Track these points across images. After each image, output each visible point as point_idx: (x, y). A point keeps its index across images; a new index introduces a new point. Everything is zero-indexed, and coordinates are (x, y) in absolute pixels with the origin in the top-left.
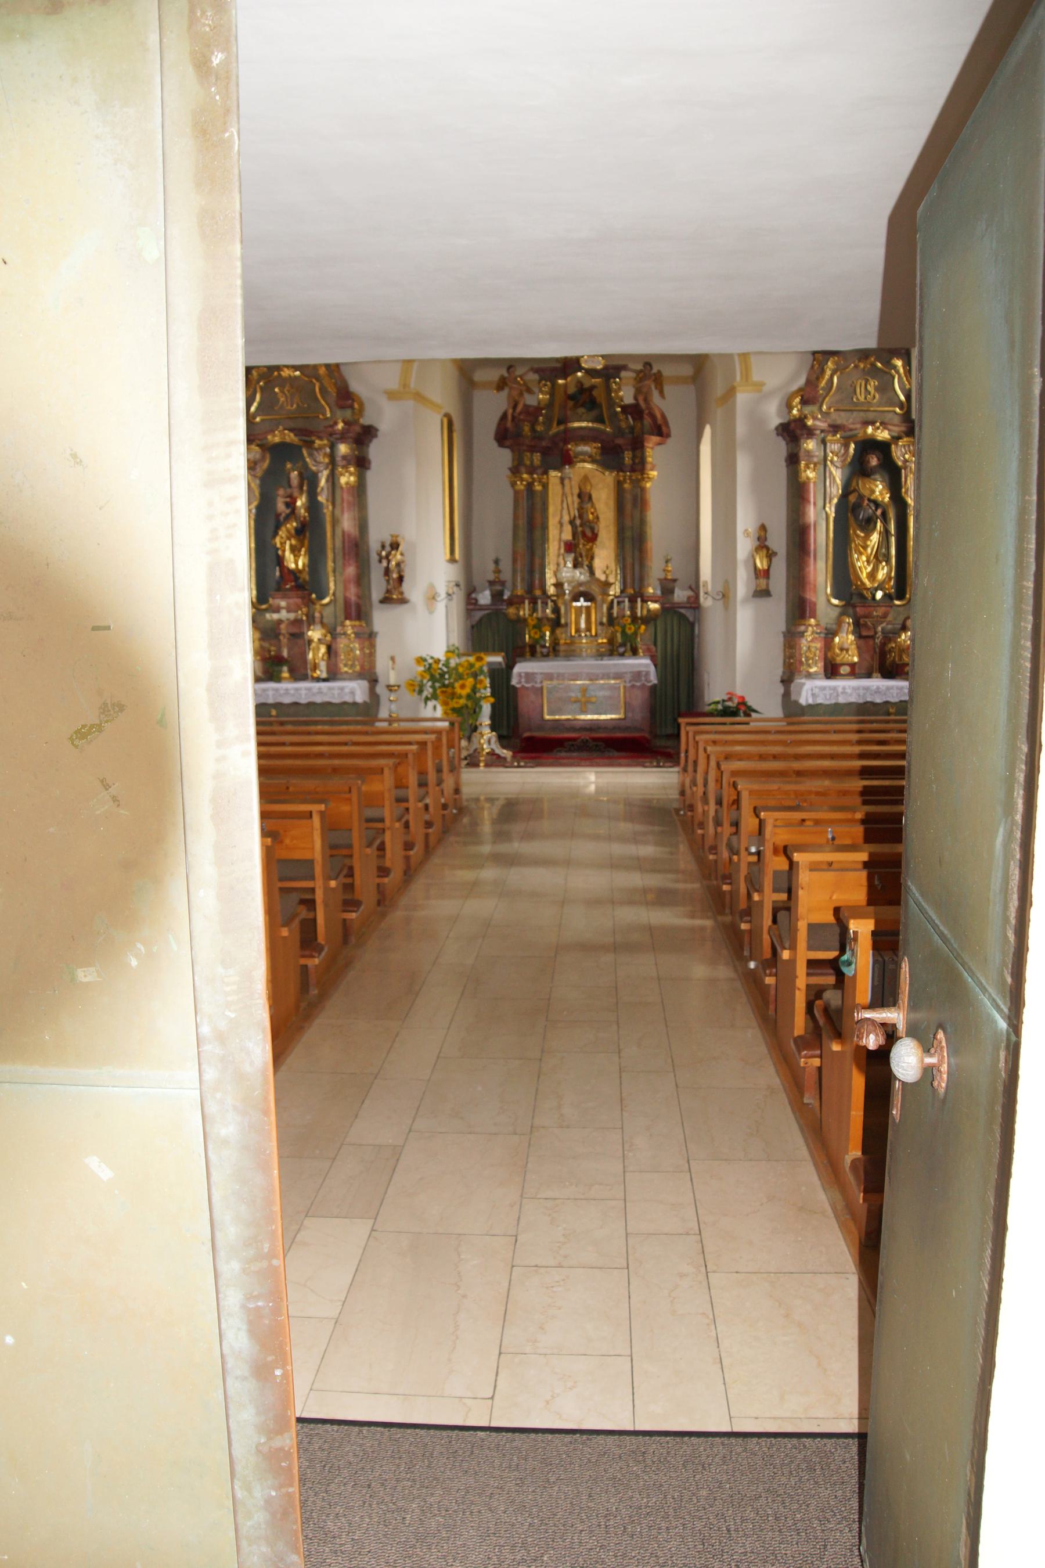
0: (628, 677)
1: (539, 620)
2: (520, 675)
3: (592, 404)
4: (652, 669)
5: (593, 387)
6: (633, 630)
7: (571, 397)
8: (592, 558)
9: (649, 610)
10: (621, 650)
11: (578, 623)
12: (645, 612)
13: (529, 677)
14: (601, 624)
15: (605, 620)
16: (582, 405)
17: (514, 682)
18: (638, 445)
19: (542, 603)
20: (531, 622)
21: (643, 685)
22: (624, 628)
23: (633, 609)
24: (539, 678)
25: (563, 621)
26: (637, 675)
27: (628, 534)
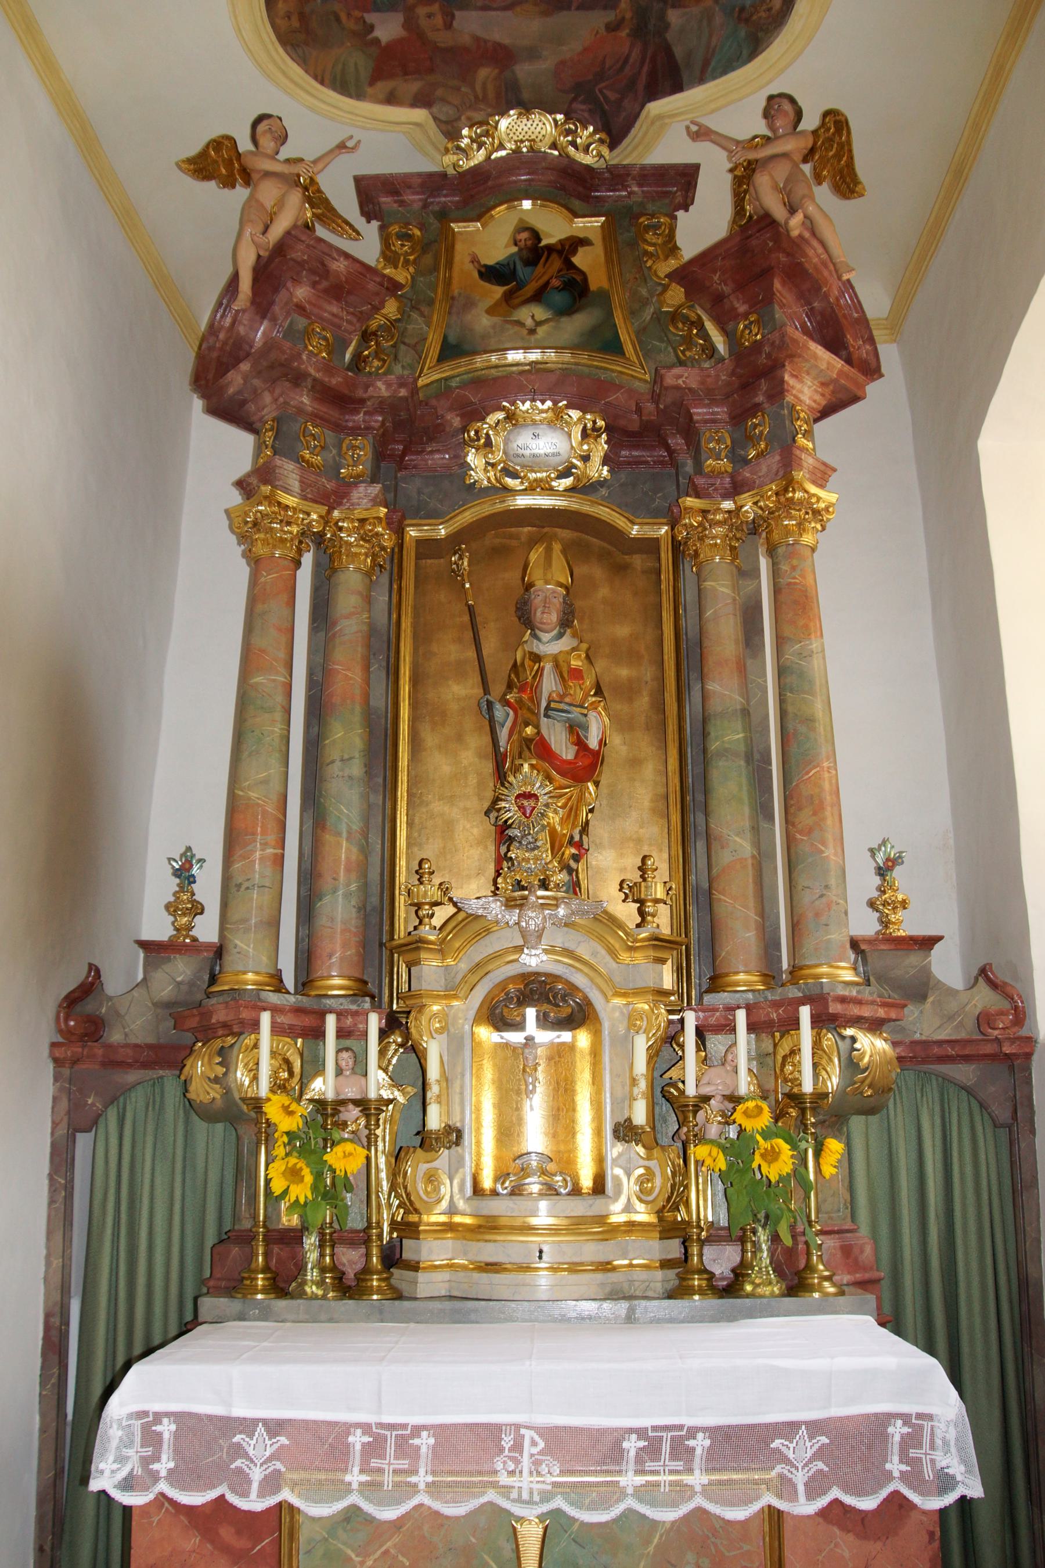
0: (801, 1450)
1: (327, 1111)
2: (148, 1424)
3: (575, 292)
4: (942, 1402)
5: (576, 243)
6: (785, 1163)
7: (492, 274)
8: (581, 851)
9: (851, 1064)
10: (721, 1260)
11: (508, 1130)
12: (833, 1082)
13: (207, 1439)
14: (625, 1131)
15: (640, 1116)
16: (537, 297)
17: (106, 1476)
18: (756, 379)
19: (342, 1033)
20: (284, 1117)
21: (897, 1504)
22: (740, 1149)
23: (774, 1065)
24: (259, 1447)
25: (434, 1121)
26: (856, 1443)
27: (728, 736)
